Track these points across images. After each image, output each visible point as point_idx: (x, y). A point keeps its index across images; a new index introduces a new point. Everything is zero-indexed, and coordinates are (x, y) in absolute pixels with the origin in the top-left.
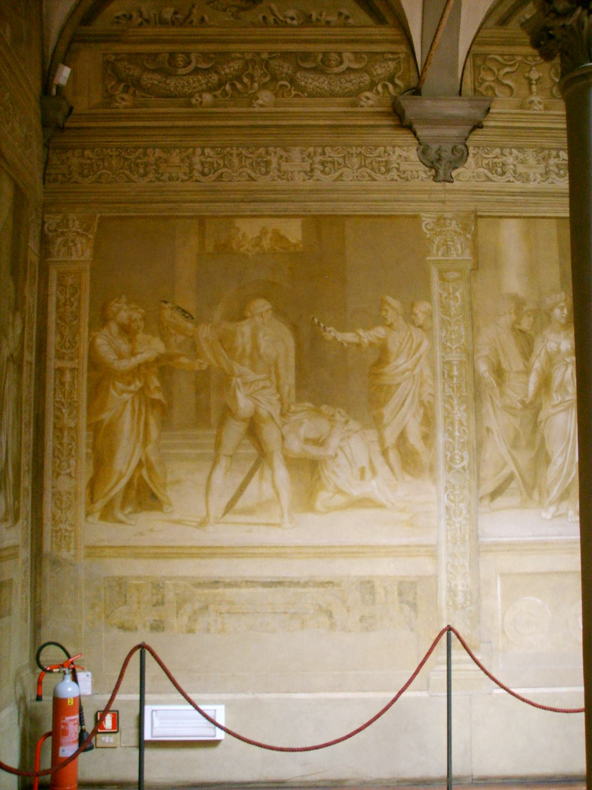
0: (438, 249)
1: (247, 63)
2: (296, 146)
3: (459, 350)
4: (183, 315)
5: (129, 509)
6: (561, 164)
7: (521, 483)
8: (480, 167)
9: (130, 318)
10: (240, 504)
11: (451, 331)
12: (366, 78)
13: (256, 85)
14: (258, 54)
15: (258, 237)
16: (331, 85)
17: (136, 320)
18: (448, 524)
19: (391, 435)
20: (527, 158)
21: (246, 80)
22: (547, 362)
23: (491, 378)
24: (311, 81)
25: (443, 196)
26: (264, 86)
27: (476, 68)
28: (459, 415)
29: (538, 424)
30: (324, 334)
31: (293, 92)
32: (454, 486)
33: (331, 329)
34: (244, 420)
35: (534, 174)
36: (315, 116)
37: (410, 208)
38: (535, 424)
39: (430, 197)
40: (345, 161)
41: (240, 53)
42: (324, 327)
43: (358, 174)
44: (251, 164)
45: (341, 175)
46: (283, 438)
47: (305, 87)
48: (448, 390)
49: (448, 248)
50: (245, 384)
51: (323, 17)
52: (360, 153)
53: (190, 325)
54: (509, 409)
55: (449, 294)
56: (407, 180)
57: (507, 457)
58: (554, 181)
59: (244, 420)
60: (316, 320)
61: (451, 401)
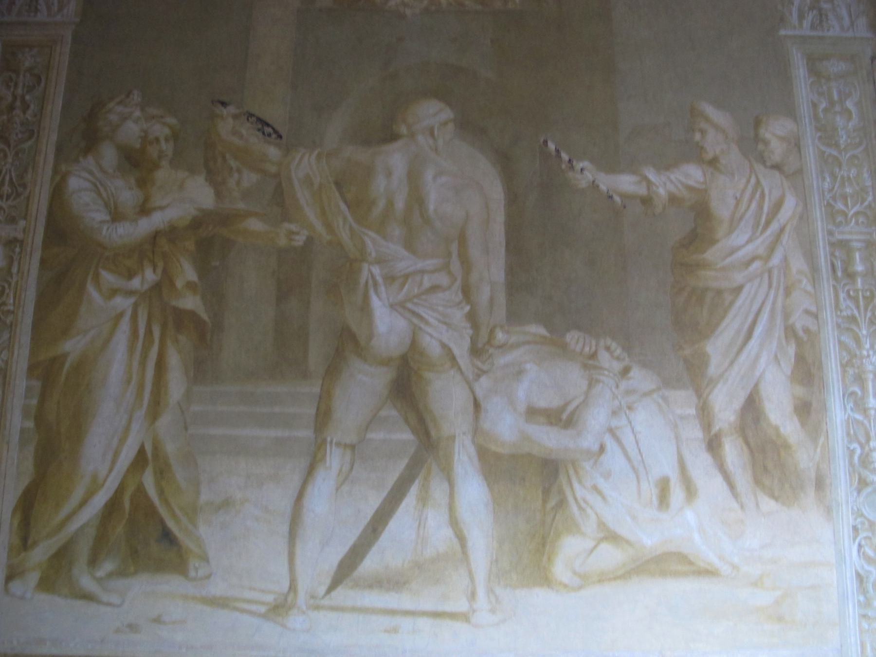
0: (801, 17)
3: (861, 219)
4: (259, 130)
5: (108, 566)
9: (145, 138)
10: (370, 564)
11: (843, 177)
17: (157, 140)
18: (864, 616)
30: (571, 174)
33: (585, 164)
34: (386, 362)
46: (477, 405)
49: (822, 16)
50: (390, 279)
53: (273, 152)
55: (832, 103)
59: (386, 362)
60: (552, 146)
61: (855, 328)
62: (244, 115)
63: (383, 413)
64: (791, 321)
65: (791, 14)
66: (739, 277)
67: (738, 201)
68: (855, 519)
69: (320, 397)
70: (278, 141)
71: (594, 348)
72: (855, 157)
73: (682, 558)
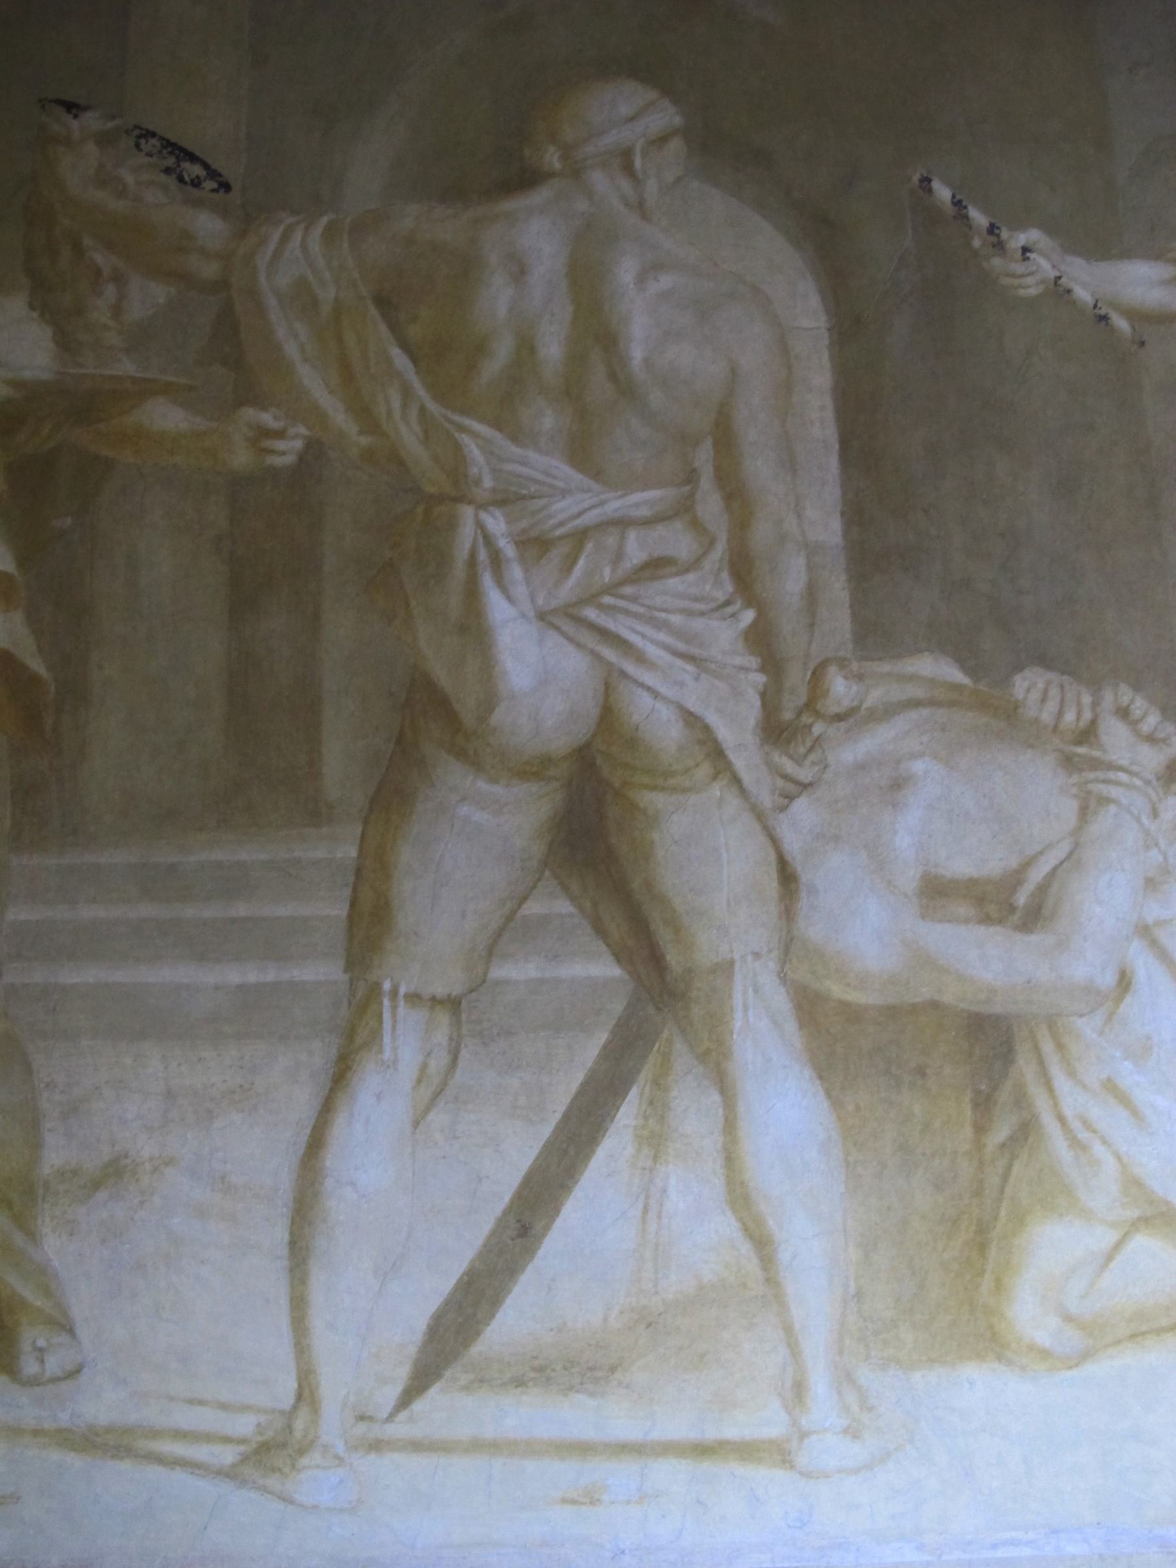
4: (167, 171)
30: (997, 262)
33: (1032, 236)
42: (992, 229)
46: (787, 876)
60: (943, 193)
62: (127, 132)
63: (533, 908)
69: (358, 872)
70: (221, 194)
71: (1087, 715)
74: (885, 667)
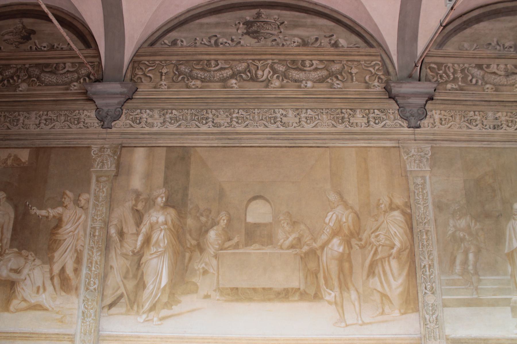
0: (98, 165)
1: (17, 69)
2: (33, 111)
3: (100, 221)
6: (173, 117)
7: (127, 299)
8: (127, 120)
12: (76, 75)
13: (20, 80)
14: (24, 65)
15: (5, 159)
16: (58, 80)
18: (83, 322)
19: (56, 269)
20: (154, 114)
21: (15, 78)
22: (149, 229)
23: (117, 237)
24: (47, 78)
25: (105, 136)
26: (24, 81)
27: (134, 68)
28: (96, 258)
29: (141, 264)
31: (38, 84)
32: (88, 299)
33: (35, 208)
35: (157, 123)
36: (46, 95)
37: (86, 143)
38: (139, 265)
39: (98, 137)
40: (57, 119)
41: (15, 65)
42: (31, 207)
43: (63, 125)
44: (10, 121)
45: (54, 126)
47: (44, 81)
48: (91, 243)
49: (103, 164)
51: (60, 46)
52: (66, 114)
54: (125, 256)
55: (100, 189)
56: (88, 128)
57: (121, 284)
58: (168, 127)
60: (28, 203)
64: (77, 248)
65: (95, 164)
66: (66, 237)
67: (70, 216)
68: (84, 298)
72: (103, 204)
73: (40, 306)
74: (11, 249)
